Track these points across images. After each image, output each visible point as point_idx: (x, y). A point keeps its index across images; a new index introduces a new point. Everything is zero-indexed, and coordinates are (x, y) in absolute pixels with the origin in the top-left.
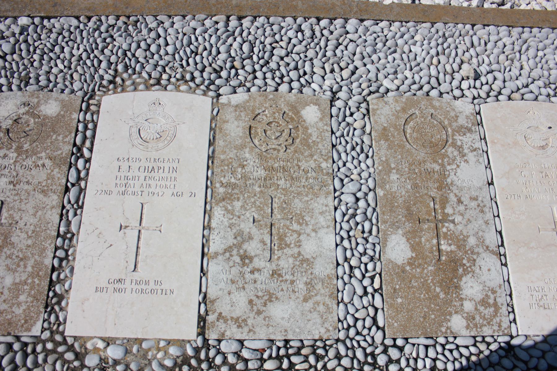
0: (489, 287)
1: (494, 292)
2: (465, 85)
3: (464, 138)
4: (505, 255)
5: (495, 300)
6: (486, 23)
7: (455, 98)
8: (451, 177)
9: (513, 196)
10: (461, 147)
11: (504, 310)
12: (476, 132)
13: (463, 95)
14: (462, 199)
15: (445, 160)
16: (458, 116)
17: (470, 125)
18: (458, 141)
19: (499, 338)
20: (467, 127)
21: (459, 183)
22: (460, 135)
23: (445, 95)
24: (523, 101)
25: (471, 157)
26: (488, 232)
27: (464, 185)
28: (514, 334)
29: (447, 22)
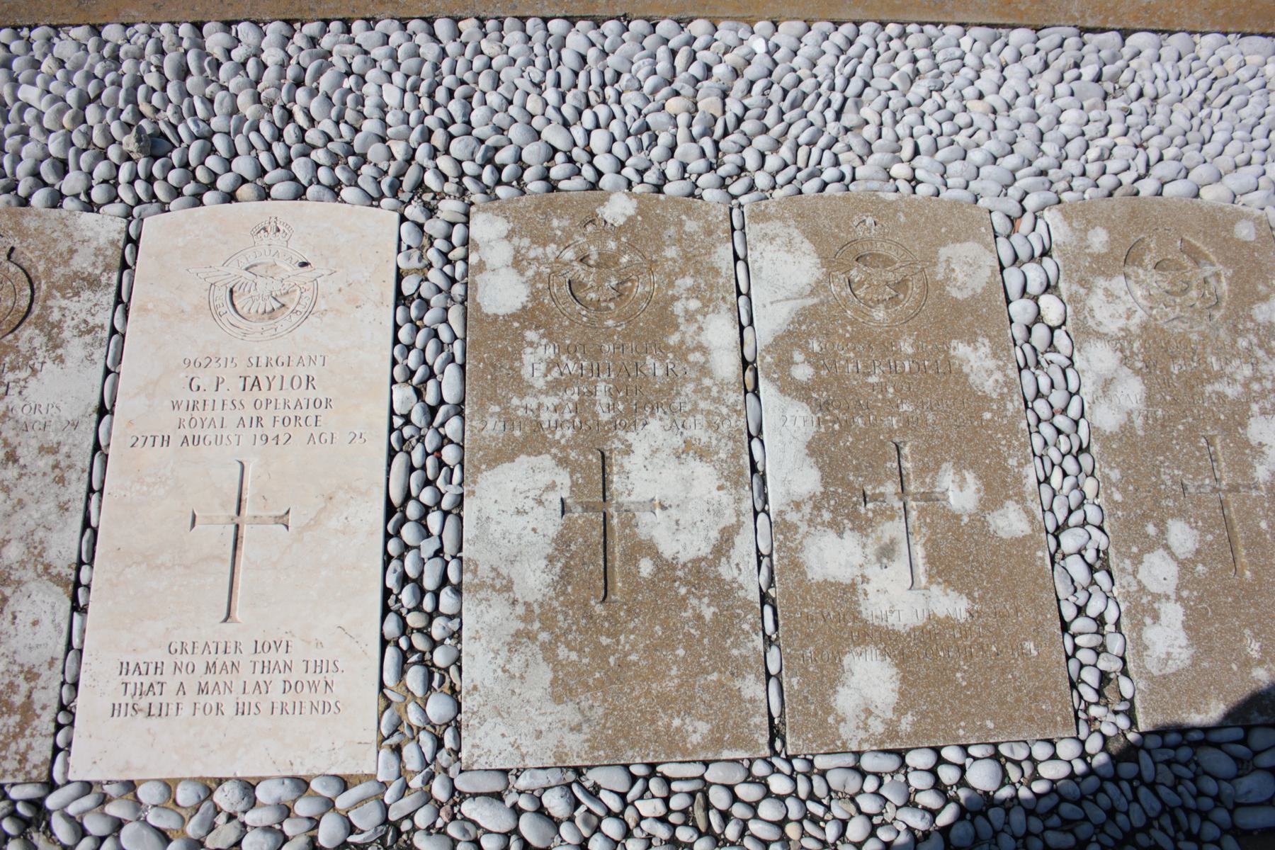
0: (22, 665)
1: (31, 675)
2: (124, 174)
3: (73, 305)
4: (88, 587)
5: (29, 697)
6: (230, 17)
7: (90, 206)
8: (7, 399)
9: (150, 440)
10: (58, 325)
11: (45, 722)
12: (109, 285)
13: (117, 196)
14: (19, 451)
15: (7, 359)
16: (76, 251)
17: (98, 272)
18: (56, 310)
19: (14, 789)
20: (90, 274)
21: (22, 416)
22: (64, 297)
23: (68, 203)
24: (269, 202)
25: (75, 348)
26: (61, 530)
27: (37, 416)
28: (58, 776)
29: (131, 20)
